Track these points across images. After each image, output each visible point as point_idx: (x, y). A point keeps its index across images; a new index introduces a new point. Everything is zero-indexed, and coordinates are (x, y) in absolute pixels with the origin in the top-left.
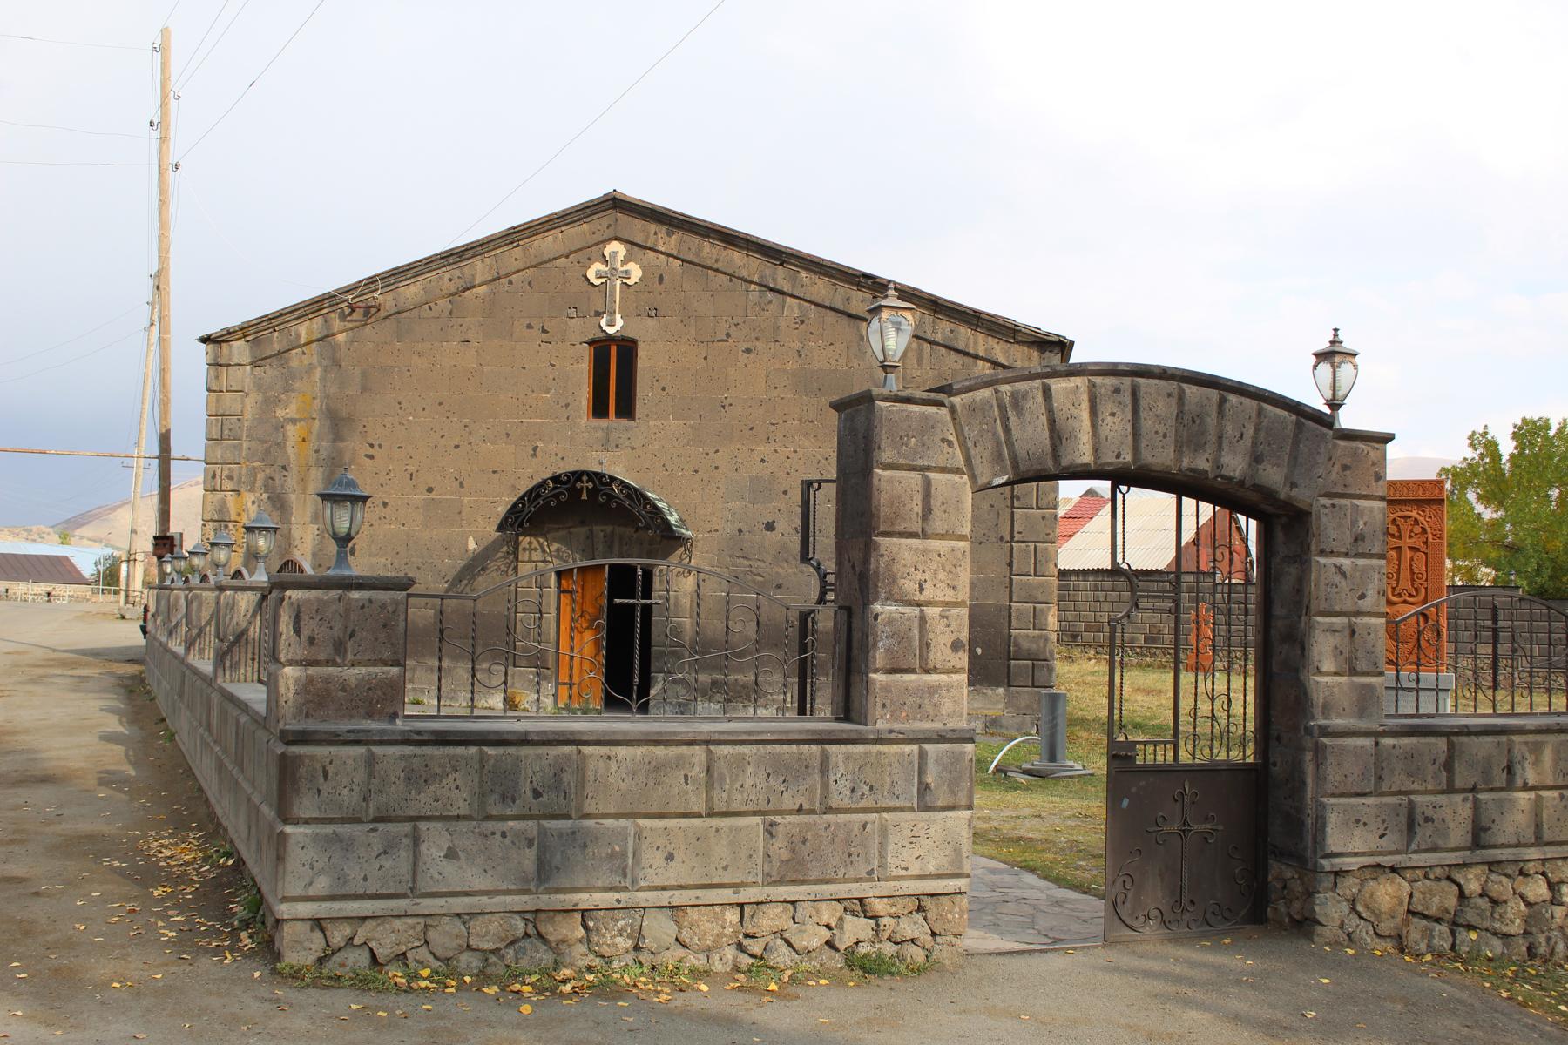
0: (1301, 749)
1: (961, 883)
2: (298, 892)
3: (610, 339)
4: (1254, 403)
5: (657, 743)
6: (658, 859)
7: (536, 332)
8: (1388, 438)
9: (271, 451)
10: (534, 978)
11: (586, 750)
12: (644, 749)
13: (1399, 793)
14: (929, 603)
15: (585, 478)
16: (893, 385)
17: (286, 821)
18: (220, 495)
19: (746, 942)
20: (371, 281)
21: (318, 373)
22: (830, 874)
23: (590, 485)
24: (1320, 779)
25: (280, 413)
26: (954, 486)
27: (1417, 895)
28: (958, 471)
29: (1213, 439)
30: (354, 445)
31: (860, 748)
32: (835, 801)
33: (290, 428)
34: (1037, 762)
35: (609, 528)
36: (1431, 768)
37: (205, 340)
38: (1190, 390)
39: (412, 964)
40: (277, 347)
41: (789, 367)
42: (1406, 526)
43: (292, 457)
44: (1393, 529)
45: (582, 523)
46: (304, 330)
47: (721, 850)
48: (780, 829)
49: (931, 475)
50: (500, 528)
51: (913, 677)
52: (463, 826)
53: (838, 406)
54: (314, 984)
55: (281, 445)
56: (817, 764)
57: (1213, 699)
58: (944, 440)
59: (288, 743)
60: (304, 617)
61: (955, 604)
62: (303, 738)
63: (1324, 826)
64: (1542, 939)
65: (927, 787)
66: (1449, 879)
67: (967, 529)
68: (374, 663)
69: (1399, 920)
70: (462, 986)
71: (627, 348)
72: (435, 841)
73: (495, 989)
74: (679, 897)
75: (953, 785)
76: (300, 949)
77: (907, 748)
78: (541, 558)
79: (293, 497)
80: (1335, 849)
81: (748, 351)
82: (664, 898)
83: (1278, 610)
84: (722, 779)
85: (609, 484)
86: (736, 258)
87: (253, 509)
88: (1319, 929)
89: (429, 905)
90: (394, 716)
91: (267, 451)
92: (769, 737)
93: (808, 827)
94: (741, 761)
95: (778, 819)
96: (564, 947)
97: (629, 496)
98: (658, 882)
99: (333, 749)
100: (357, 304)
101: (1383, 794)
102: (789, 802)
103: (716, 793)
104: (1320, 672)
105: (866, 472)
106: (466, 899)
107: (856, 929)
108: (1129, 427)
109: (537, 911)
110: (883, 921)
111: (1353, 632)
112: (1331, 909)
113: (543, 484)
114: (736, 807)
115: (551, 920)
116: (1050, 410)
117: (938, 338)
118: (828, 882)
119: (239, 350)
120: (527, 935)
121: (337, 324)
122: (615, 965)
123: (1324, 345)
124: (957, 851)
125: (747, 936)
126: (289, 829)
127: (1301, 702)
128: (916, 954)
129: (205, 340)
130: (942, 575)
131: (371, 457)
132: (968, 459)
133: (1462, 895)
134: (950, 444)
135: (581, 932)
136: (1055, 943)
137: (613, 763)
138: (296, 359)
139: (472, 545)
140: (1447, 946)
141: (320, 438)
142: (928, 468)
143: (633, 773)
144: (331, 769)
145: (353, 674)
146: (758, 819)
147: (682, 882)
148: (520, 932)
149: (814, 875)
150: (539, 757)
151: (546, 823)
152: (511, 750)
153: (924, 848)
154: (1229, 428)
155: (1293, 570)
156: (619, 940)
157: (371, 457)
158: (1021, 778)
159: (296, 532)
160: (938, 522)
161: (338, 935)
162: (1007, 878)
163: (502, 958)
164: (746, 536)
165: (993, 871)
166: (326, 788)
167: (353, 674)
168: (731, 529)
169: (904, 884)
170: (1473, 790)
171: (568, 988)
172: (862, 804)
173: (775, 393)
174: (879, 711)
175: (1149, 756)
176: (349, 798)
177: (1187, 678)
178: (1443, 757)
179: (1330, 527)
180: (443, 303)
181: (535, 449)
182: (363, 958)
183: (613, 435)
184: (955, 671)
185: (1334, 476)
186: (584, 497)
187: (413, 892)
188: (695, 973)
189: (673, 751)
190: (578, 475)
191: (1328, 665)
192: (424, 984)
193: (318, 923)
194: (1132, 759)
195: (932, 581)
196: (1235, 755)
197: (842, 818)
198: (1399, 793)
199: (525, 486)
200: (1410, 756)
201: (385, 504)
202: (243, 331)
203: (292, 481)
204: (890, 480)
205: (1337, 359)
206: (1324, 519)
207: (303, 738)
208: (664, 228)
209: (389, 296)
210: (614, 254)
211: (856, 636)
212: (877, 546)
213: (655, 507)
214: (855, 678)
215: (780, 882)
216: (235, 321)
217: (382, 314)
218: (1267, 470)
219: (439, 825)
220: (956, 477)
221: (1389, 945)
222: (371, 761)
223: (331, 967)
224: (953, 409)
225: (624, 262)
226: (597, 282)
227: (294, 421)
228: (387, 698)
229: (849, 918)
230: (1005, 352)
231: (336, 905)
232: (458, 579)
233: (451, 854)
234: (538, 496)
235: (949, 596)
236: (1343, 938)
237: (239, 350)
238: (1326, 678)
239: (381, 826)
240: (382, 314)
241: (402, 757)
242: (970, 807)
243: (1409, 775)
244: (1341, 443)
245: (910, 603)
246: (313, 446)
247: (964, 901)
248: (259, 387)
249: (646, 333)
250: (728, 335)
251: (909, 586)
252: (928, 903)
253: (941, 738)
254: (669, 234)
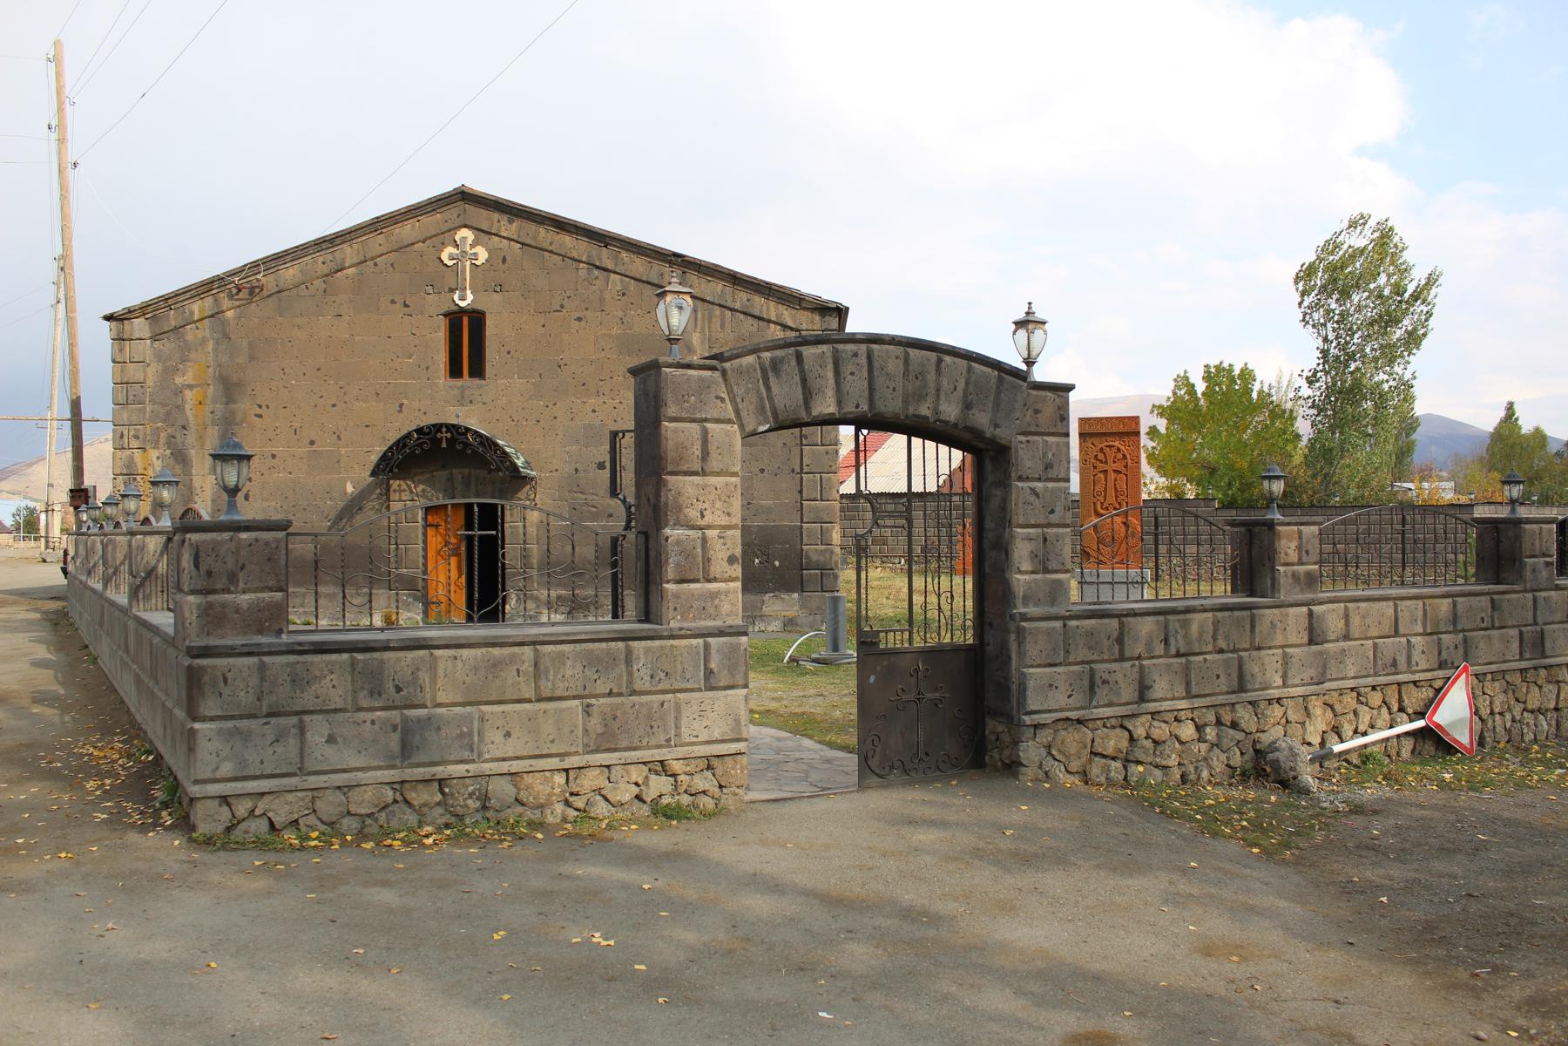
0: (1007, 631)
1: (741, 746)
2: (208, 775)
3: (463, 311)
4: (965, 362)
5: (494, 645)
6: (498, 737)
7: (399, 306)
8: (1070, 388)
9: (172, 414)
10: (402, 835)
11: (437, 652)
12: (484, 650)
13: (1083, 662)
14: (709, 527)
16: (677, 354)
17: (195, 719)
18: (128, 452)
19: (572, 799)
20: (255, 265)
21: (210, 345)
22: (636, 743)
24: (1022, 654)
25: (179, 380)
26: (727, 433)
27: (1098, 740)
28: (729, 421)
29: (932, 391)
30: (244, 406)
31: (657, 643)
32: (638, 686)
33: (188, 394)
34: (824, 652)
35: (466, 471)
36: (1106, 643)
37: (108, 318)
38: (913, 352)
39: (303, 829)
40: (173, 323)
41: (613, 332)
42: (1110, 453)
43: (191, 418)
44: (1101, 456)
45: (443, 467)
46: (196, 308)
47: (548, 728)
48: (595, 709)
49: (708, 425)
50: (374, 473)
51: (697, 585)
52: (340, 717)
53: (634, 372)
54: (224, 847)
55: (180, 408)
56: (623, 657)
57: (939, 596)
58: (717, 397)
59: (194, 657)
60: (202, 554)
61: (730, 527)
62: (206, 652)
63: (1025, 690)
64: (1191, 768)
65: (711, 671)
66: (1122, 726)
67: (737, 468)
68: (262, 590)
69: (1084, 759)
70: (344, 843)
71: (477, 319)
72: (318, 730)
73: (372, 844)
74: (516, 766)
75: (732, 669)
76: (209, 819)
77: (694, 642)
78: (410, 498)
79: (193, 452)
80: (1034, 708)
81: (579, 319)
82: (505, 767)
83: (989, 524)
84: (547, 672)
86: (567, 240)
87: (158, 464)
88: (1023, 769)
89: (314, 781)
90: (280, 632)
91: (168, 414)
92: (583, 637)
93: (618, 707)
94: (562, 657)
95: (593, 701)
96: (425, 810)
97: (481, 444)
98: (499, 755)
99: (230, 660)
100: (242, 285)
101: (1070, 664)
102: (602, 687)
103: (542, 683)
104: (1020, 572)
105: (657, 424)
106: (346, 775)
107: (659, 785)
108: (866, 383)
109: (403, 782)
110: (680, 778)
111: (1045, 540)
112: (1030, 751)
113: (409, 435)
114: (559, 693)
115: (414, 789)
116: (802, 371)
117: (737, 306)
118: (635, 749)
119: (139, 326)
120: (395, 801)
121: (226, 303)
122: (468, 821)
123: (1021, 316)
124: (737, 721)
125: (572, 794)
126: (197, 726)
127: (1007, 595)
128: (707, 802)
129: (108, 318)
130: (718, 504)
131: (260, 416)
132: (737, 412)
133: (1132, 739)
134: (723, 400)
135: (439, 797)
136: (823, 791)
137: (459, 662)
138: (190, 333)
139: (350, 489)
140: (1121, 777)
141: (214, 402)
142: (706, 420)
143: (476, 669)
144: (230, 676)
145: (245, 599)
146: (577, 702)
147: (519, 754)
148: (390, 799)
149: (624, 744)
150: (399, 660)
151: (406, 712)
152: (377, 655)
153: (706, 719)
154: (945, 382)
155: (998, 492)
156: (470, 802)
157: (260, 416)
158: (810, 666)
159: (197, 482)
160: (715, 462)
161: (242, 809)
162: (790, 743)
163: (376, 820)
164: (582, 474)
165: (779, 739)
166: (226, 691)
167: (245, 599)
168: (568, 469)
169: (696, 748)
170: (1139, 658)
171: (430, 841)
172: (660, 687)
173: (602, 354)
174: (671, 613)
175: (890, 641)
176: (245, 698)
177: (918, 582)
178: (1116, 634)
179: (1026, 456)
180: (318, 283)
181: (401, 405)
182: (263, 825)
183: (467, 393)
184: (732, 579)
185: (1028, 418)
186: (444, 445)
187: (302, 771)
188: (530, 824)
189: (507, 651)
190: (438, 427)
191: (1026, 566)
192: (313, 843)
193: (225, 800)
194: (876, 644)
195: (712, 509)
196: (959, 638)
197: (644, 698)
198: (1083, 662)
199: (394, 437)
200: (1090, 634)
201: (274, 456)
202: (144, 309)
203: (191, 439)
204: (675, 431)
205: (1031, 326)
206: (1021, 452)
207: (206, 652)
208: (505, 217)
209: (271, 278)
211: (652, 554)
212: (665, 483)
213: (504, 452)
214: (653, 588)
215: (597, 751)
216: (135, 300)
217: (265, 293)
218: (987, 411)
219: (320, 717)
220: (728, 427)
221: (1076, 780)
222: (262, 668)
223: (237, 834)
224: (724, 373)
225: (472, 246)
226: (450, 263)
227: (191, 387)
228: (274, 618)
229: (653, 777)
230: (793, 317)
231: (239, 785)
232: (340, 517)
233: (331, 740)
234: (405, 445)
235: (725, 521)
236: (1041, 775)
237: (139, 326)
238: (1022, 578)
239: (273, 720)
240: (265, 293)
241: (288, 664)
242: (746, 686)
243: (1090, 648)
244: (1034, 392)
245: (693, 527)
246: (209, 408)
247: (744, 760)
248: (159, 357)
249: (492, 306)
251: (693, 513)
252: (715, 762)
253: (721, 633)
254: (511, 222)
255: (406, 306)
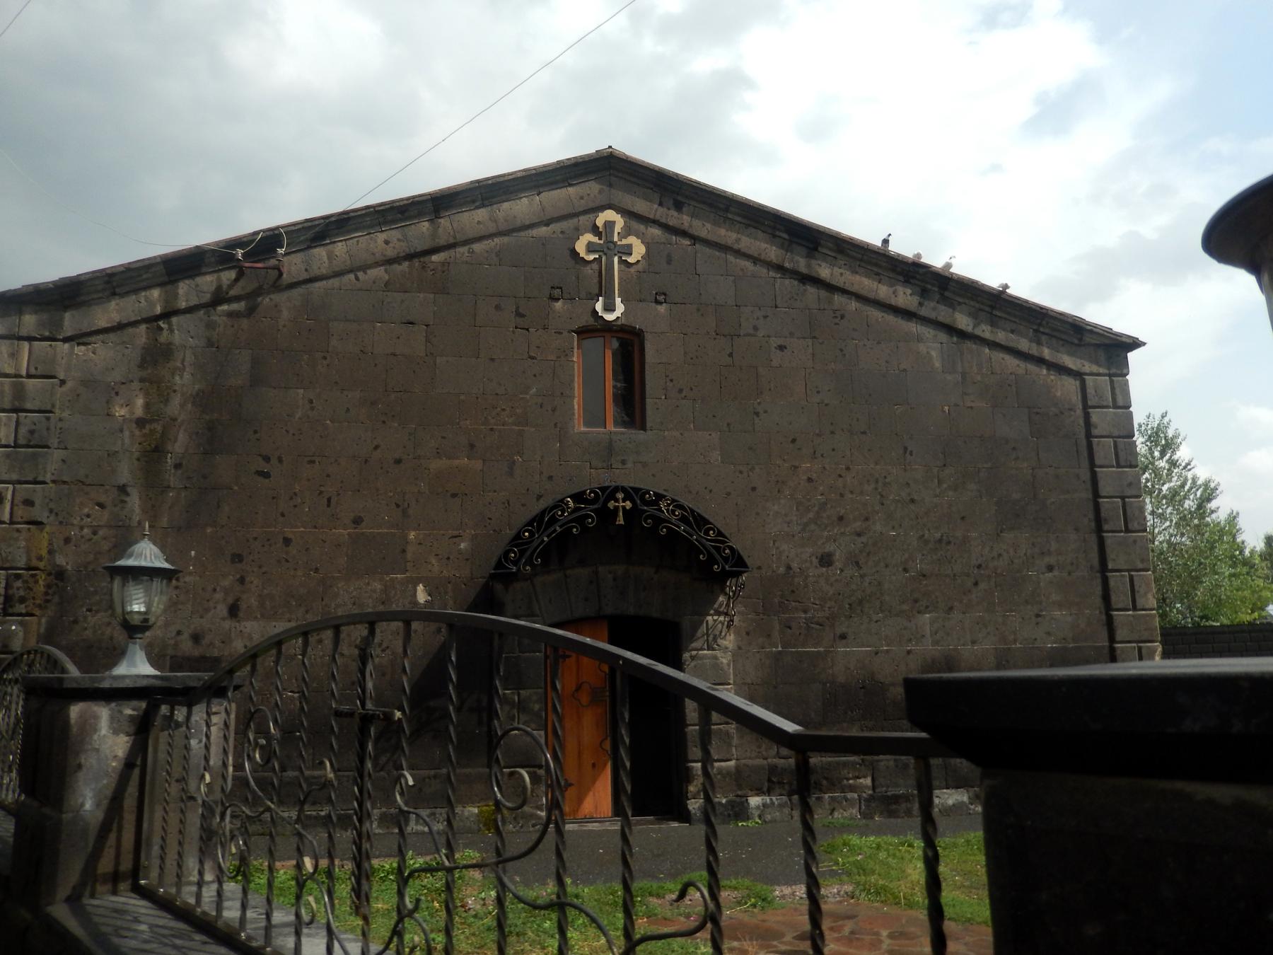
15: (620, 496)
23: (628, 505)
71: (628, 343)
81: (782, 348)
85: (656, 503)
97: (684, 519)
113: (560, 504)
131: (266, 475)
157: (266, 475)
190: (611, 493)
201: (287, 541)
209: (297, 259)
210: (610, 225)
234: (553, 520)
250: (755, 328)
255: (519, 314)
